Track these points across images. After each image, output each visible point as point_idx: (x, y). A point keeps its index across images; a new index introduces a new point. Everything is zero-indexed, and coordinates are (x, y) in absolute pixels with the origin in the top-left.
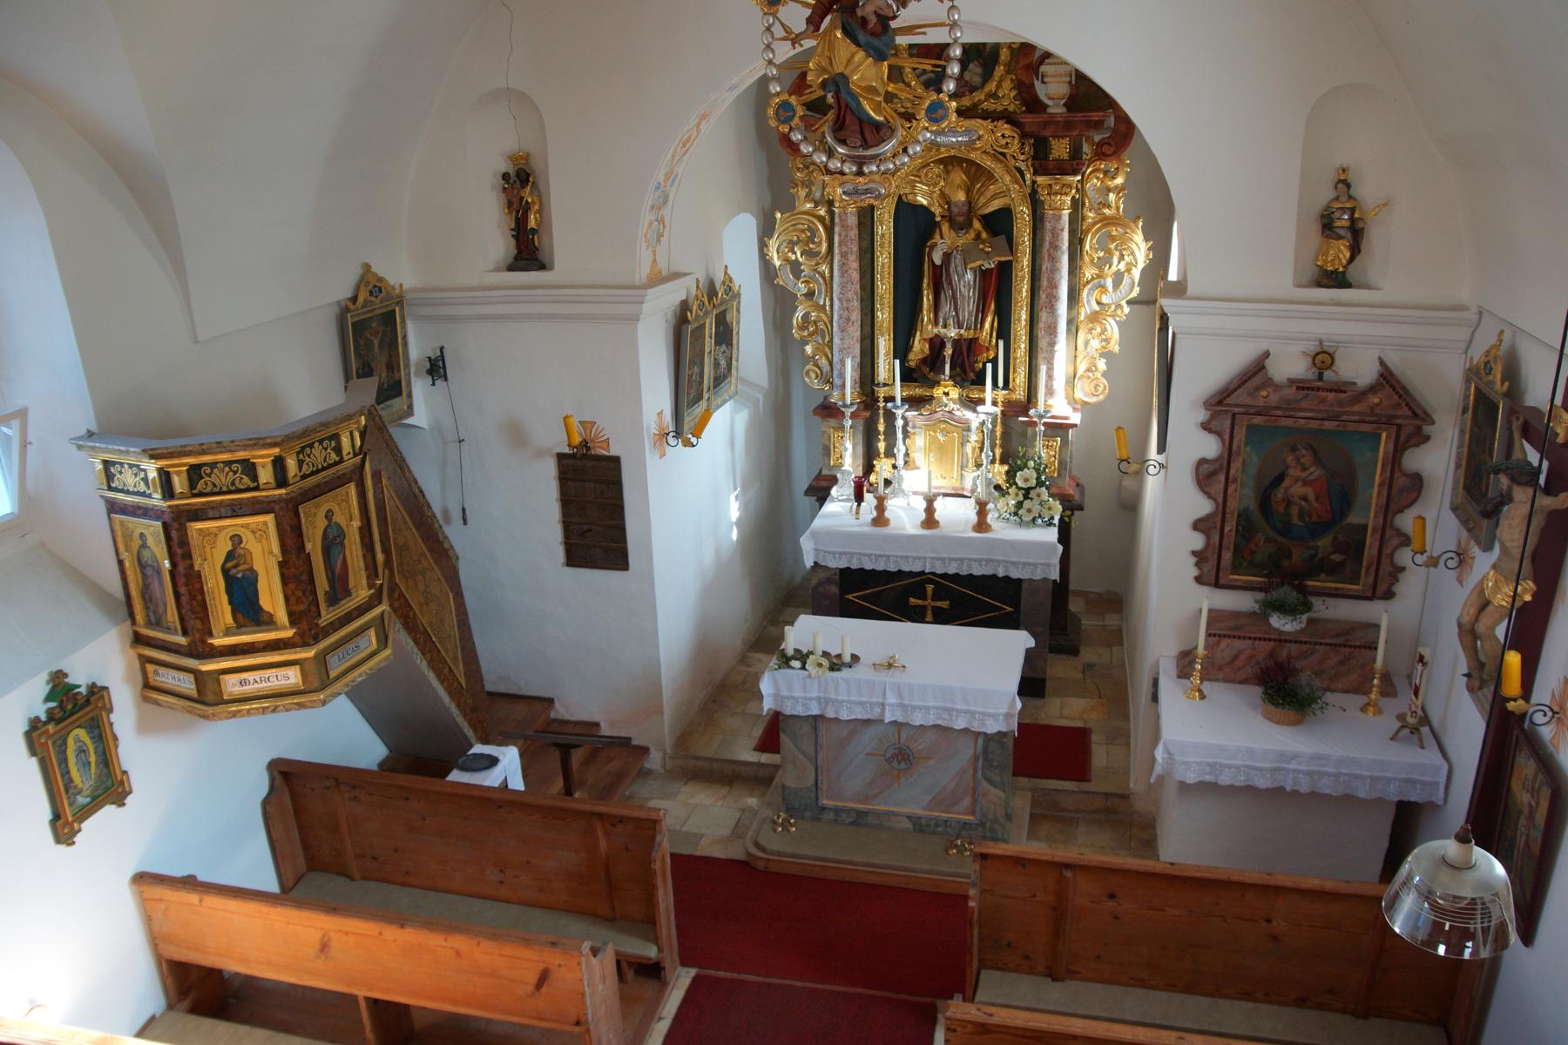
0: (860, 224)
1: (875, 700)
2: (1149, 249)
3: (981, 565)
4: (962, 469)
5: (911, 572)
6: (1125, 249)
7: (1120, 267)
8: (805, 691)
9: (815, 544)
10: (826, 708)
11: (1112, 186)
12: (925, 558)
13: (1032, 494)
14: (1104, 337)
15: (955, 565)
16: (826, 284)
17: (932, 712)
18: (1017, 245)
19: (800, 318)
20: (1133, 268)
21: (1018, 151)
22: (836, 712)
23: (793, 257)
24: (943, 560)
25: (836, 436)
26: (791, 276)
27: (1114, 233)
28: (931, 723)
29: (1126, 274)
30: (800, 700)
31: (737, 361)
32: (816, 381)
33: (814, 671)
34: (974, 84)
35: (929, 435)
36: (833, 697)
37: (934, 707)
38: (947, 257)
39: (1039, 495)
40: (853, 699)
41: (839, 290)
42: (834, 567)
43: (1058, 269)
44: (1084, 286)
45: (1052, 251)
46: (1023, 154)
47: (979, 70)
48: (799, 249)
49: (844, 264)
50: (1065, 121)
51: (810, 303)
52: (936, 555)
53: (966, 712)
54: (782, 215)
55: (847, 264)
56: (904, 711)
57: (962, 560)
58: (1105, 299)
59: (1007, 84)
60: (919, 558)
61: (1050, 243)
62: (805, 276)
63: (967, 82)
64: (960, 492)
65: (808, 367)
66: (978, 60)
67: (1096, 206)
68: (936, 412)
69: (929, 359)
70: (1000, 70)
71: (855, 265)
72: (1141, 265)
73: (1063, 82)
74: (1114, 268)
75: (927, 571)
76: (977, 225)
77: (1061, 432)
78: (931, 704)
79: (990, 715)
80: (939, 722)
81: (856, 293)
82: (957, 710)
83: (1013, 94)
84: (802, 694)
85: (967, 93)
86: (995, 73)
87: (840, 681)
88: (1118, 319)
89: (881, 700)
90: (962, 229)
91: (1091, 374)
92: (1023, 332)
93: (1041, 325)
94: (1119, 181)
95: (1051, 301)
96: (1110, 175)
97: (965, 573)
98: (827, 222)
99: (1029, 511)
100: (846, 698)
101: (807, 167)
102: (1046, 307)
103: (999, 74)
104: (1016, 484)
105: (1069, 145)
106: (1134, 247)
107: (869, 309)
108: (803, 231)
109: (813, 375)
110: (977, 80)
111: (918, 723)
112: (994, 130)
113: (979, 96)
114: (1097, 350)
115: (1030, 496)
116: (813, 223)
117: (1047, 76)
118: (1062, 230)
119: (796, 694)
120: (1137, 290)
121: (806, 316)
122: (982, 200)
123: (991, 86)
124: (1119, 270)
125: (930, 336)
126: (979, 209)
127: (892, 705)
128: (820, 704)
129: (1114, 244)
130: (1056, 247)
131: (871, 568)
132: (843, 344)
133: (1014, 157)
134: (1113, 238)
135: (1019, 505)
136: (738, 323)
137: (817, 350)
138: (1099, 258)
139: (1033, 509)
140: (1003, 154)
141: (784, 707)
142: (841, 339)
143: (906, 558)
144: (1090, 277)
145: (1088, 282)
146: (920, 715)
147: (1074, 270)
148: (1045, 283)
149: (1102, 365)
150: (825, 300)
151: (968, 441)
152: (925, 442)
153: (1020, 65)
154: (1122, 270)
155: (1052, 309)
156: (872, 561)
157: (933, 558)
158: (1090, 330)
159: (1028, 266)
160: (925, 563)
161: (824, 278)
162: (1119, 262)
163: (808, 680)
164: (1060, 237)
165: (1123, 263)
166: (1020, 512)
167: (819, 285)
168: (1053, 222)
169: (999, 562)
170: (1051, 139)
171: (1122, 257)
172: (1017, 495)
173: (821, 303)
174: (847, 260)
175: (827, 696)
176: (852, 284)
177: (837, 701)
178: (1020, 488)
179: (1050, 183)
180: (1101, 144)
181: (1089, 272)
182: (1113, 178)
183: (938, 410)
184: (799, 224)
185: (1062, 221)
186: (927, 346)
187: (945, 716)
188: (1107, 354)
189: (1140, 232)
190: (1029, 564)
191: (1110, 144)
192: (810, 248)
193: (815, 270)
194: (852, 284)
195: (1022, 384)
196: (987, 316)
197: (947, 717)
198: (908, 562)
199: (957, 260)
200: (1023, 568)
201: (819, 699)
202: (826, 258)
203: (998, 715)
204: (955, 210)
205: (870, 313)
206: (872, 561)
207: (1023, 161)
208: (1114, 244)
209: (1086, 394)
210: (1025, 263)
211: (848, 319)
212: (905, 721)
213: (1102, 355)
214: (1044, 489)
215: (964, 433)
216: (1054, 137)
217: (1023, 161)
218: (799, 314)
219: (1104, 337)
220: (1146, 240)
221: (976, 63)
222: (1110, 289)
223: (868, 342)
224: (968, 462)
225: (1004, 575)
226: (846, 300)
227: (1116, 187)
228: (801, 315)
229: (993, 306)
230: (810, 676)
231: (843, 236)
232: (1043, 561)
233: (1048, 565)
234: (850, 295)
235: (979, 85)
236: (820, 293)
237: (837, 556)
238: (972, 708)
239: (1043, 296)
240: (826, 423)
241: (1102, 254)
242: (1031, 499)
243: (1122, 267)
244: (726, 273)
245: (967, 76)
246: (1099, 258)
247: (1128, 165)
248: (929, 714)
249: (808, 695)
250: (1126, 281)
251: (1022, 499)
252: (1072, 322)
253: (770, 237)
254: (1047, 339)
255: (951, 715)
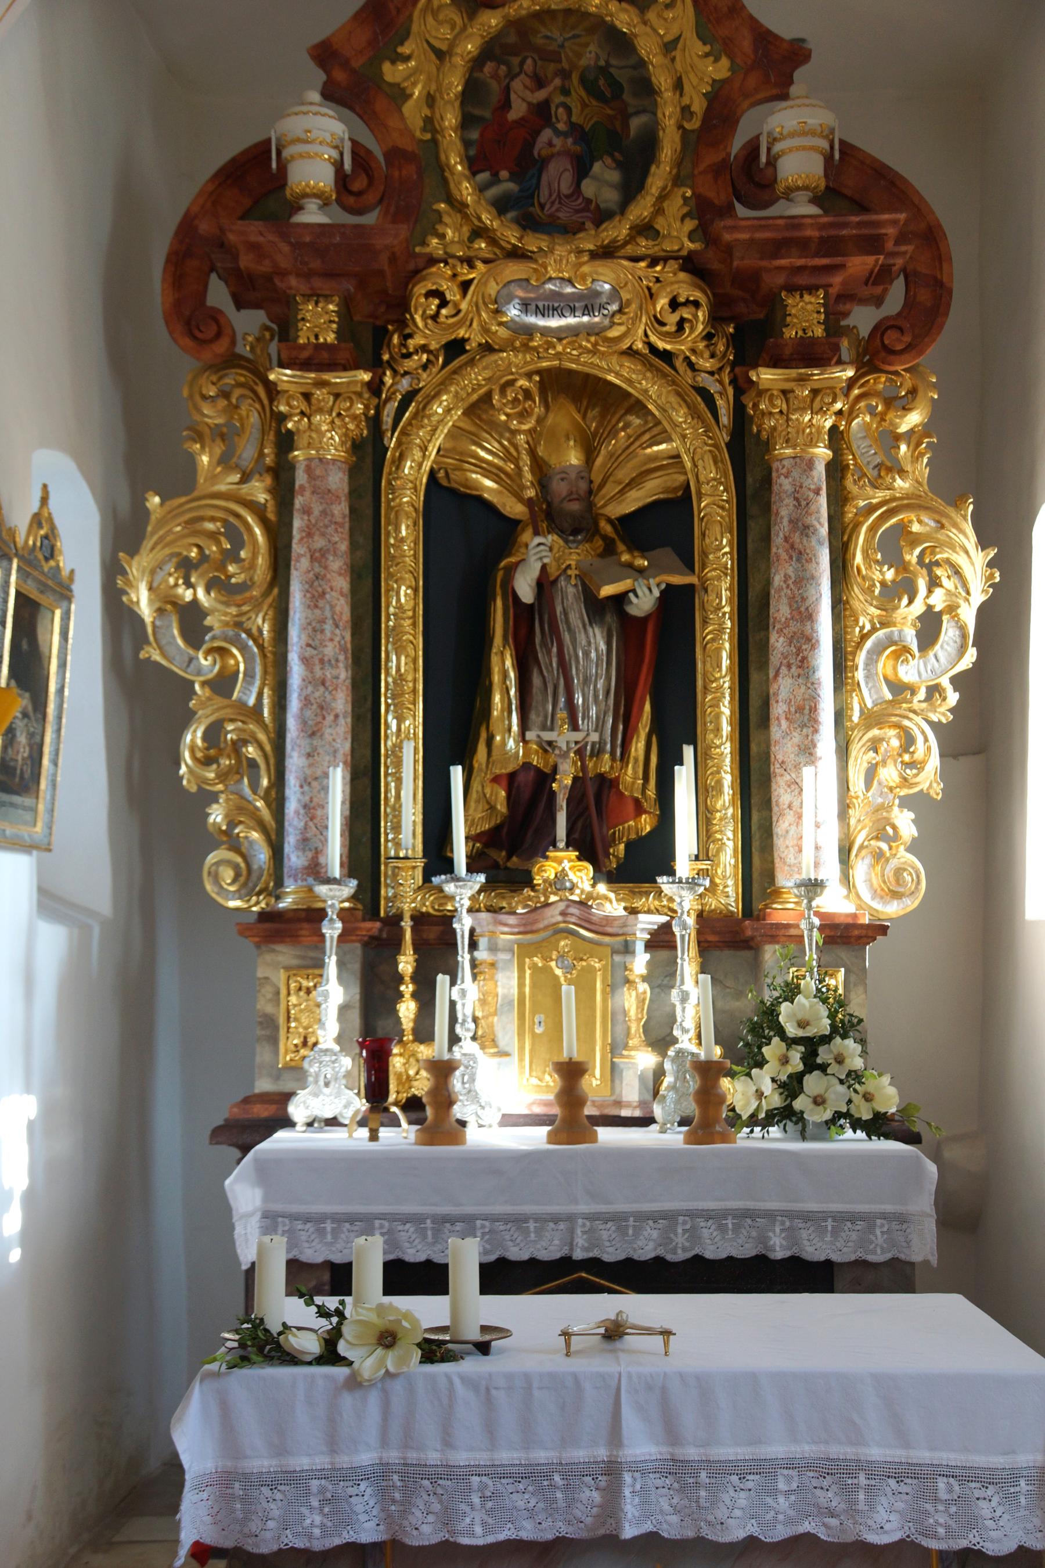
0: (354, 493)
1: (580, 1454)
2: (991, 564)
3: (722, 1229)
4: (612, 1052)
5: (533, 1262)
6: (937, 564)
7: (930, 601)
8: (333, 1445)
9: (266, 1198)
10: (404, 1513)
11: (903, 428)
12: (570, 1218)
13: (824, 1055)
14: (907, 758)
15: (655, 1234)
16: (264, 656)
17: (782, 1486)
18: (705, 554)
19: (199, 742)
20: (961, 602)
21: (701, 345)
22: (447, 1518)
23: (188, 595)
24: (618, 1219)
25: (293, 985)
26: (180, 642)
27: (916, 528)
28: (781, 1533)
29: (945, 618)
30: (315, 1484)
31: (55, 763)
32: (232, 888)
33: (369, 1362)
34: (602, 206)
35: (534, 967)
36: (433, 1457)
37: (790, 1464)
38: (544, 585)
39: (840, 1060)
40: (506, 1456)
41: (304, 637)
42: (319, 1259)
43: (813, 577)
44: (859, 645)
45: (796, 538)
46: (712, 356)
47: (614, 176)
48: (200, 576)
49: (317, 577)
50: (821, 238)
51: (220, 701)
52: (603, 1208)
53: (902, 1472)
54: (162, 503)
55: (324, 577)
56: (683, 1489)
57: (670, 1217)
58: (909, 672)
59: (675, 206)
60: (556, 1219)
61: (791, 521)
62: (214, 638)
63: (589, 201)
64: (613, 1112)
65: (212, 858)
66: (612, 156)
67: (871, 473)
68: (547, 905)
69: (505, 830)
70: (658, 178)
71: (343, 583)
72: (978, 597)
73: (812, 148)
74: (918, 608)
75: (578, 1255)
76: (607, 528)
77: (843, 953)
78: (777, 1450)
79: (987, 1478)
80: (807, 1527)
81: (343, 649)
82: (859, 1466)
83: (690, 225)
84: (322, 1461)
85: (589, 225)
86: (650, 180)
87: (457, 1381)
88: (934, 718)
89: (602, 1453)
90: (575, 532)
91: (884, 846)
92: (727, 749)
93: (778, 709)
94: (913, 419)
95: (799, 650)
96: (899, 403)
97: (681, 1256)
98: (271, 516)
99: (819, 1101)
100: (481, 1457)
101: (225, 395)
102: (789, 666)
103: (660, 184)
104: (781, 1032)
105: (824, 305)
106: (960, 559)
107: (369, 704)
108: (213, 536)
109: (228, 874)
110: (610, 197)
111: (737, 1533)
112: (655, 287)
113: (618, 230)
114: (891, 789)
115: (819, 1061)
116: (238, 516)
117: (782, 138)
118: (817, 492)
119: (302, 1462)
120: (971, 655)
121: (213, 734)
122: (611, 489)
123: (641, 209)
124: (930, 608)
125: (510, 768)
126: (605, 506)
127: (640, 1468)
128: (384, 1494)
129: (917, 551)
130: (807, 527)
131: (421, 1257)
132: (310, 765)
133: (691, 365)
134: (915, 540)
135: (791, 1087)
136: (62, 665)
137: (241, 811)
138: (883, 584)
139: (830, 1096)
140: (666, 356)
141: (254, 1526)
142: (309, 755)
143: (519, 1221)
144: (868, 627)
145: (864, 637)
146: (742, 1498)
147: (839, 605)
148: (780, 610)
149: (905, 823)
150: (260, 695)
151: (627, 981)
152: (521, 985)
153: (702, 167)
154: (937, 609)
155: (804, 666)
156: (424, 1237)
157: (592, 1217)
158: (874, 746)
159: (730, 601)
160: (572, 1231)
161: (261, 647)
162: (930, 591)
163: (348, 1401)
164: (813, 508)
165: (938, 592)
166: (798, 1104)
167: (248, 659)
168: (795, 474)
169: (770, 1216)
170: (783, 294)
171: (934, 583)
172: (785, 1061)
173: (252, 701)
174: (326, 568)
175: (412, 1456)
176: (337, 626)
177: (449, 1471)
178: (792, 1042)
179: (787, 386)
180: (880, 329)
181: (866, 614)
182: (906, 409)
183: (553, 898)
184: (202, 519)
185: (815, 473)
186: (503, 793)
187: (830, 1498)
188: (915, 802)
189: (969, 528)
190: (853, 1218)
191: (901, 330)
192: (230, 577)
193: (238, 625)
194: (337, 626)
195: (729, 871)
196: (636, 729)
197: (836, 1503)
198: (526, 1232)
199: (569, 592)
200: (835, 1232)
201: (381, 1473)
202: (266, 593)
203: (1014, 1476)
204: (559, 488)
205: (369, 716)
206: (424, 1237)
207: (712, 373)
208: (917, 551)
209: (875, 894)
210: (725, 594)
211: (323, 708)
212: (690, 1534)
213: (906, 803)
214: (850, 1043)
215: (617, 958)
216: (791, 289)
217: (712, 373)
218: (194, 736)
219: (907, 758)
220: (983, 543)
221: (608, 160)
222: (914, 647)
223: (367, 781)
224: (628, 1034)
225: (788, 1254)
226: (322, 661)
227: (911, 431)
228: (199, 734)
229: (647, 707)
230: (354, 1383)
231: (317, 509)
232: (889, 1208)
233: (902, 1219)
234: (330, 650)
235: (614, 207)
236: (249, 675)
237: (329, 1226)
238: (923, 1455)
239: (778, 643)
240: (268, 957)
241: (890, 575)
242: (823, 1068)
243: (938, 600)
244: (44, 500)
245: (588, 188)
246: (883, 584)
247: (934, 386)
248: (774, 1493)
249: (344, 1461)
250: (949, 633)
251: (801, 1067)
252: (840, 716)
253: (133, 551)
254: (797, 738)
255: (848, 1492)
